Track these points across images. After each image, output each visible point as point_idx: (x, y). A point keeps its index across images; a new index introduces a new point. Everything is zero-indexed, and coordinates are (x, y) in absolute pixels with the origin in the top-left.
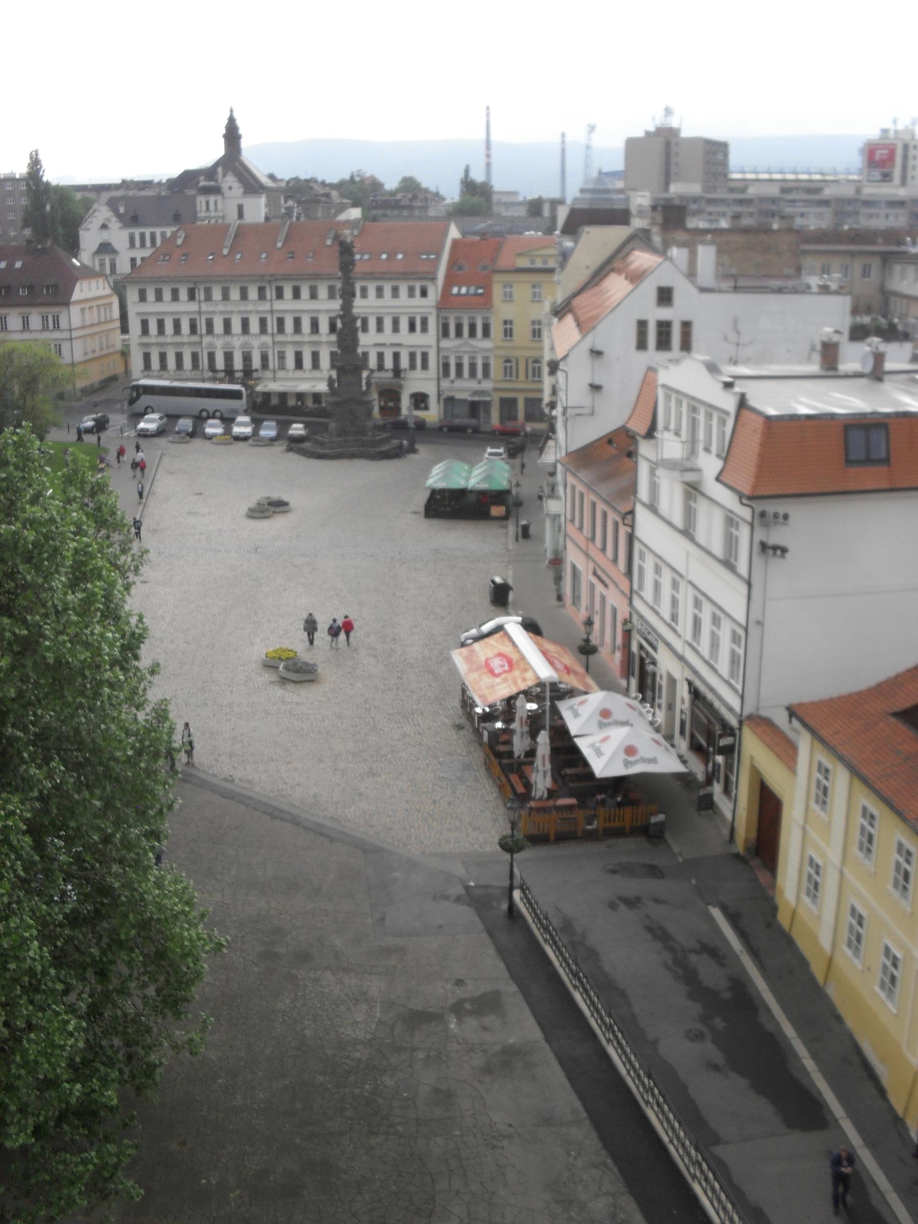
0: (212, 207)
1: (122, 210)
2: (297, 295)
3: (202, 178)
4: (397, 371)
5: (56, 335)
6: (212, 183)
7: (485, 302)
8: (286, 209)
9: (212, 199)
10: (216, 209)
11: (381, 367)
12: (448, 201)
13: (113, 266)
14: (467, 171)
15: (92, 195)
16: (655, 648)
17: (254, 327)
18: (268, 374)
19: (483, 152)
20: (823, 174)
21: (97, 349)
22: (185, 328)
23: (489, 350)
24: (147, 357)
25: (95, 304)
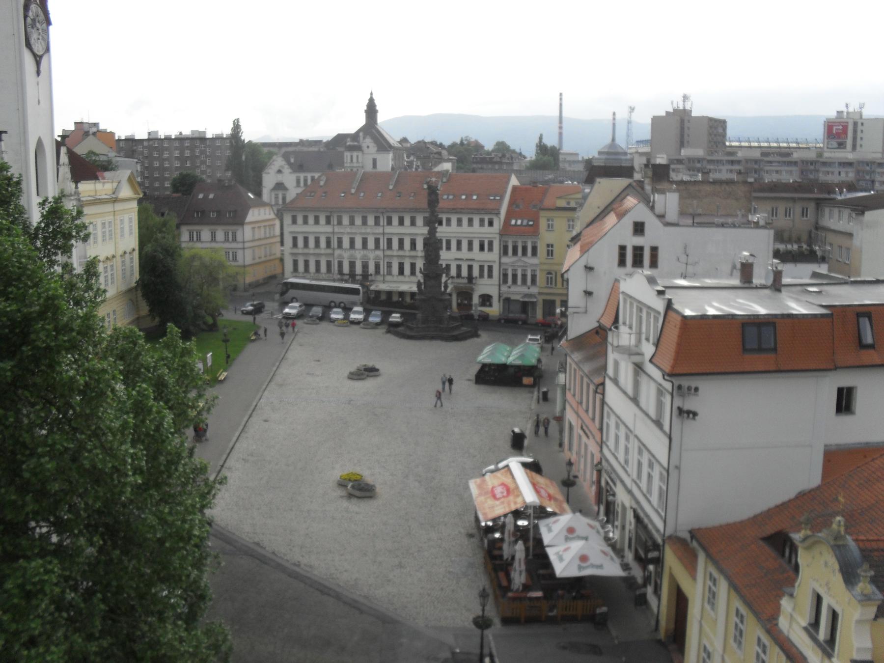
0: (355, 160)
1: (292, 160)
2: (401, 222)
3: (349, 139)
4: (470, 278)
5: (234, 245)
6: (356, 143)
7: (534, 230)
8: (407, 162)
9: (355, 154)
11: (459, 275)
12: (528, 159)
14: (541, 138)
15: (272, 149)
16: (615, 484)
17: (371, 244)
18: (380, 278)
19: (557, 124)
20: (797, 143)
22: (323, 244)
23: (536, 265)
24: (295, 263)
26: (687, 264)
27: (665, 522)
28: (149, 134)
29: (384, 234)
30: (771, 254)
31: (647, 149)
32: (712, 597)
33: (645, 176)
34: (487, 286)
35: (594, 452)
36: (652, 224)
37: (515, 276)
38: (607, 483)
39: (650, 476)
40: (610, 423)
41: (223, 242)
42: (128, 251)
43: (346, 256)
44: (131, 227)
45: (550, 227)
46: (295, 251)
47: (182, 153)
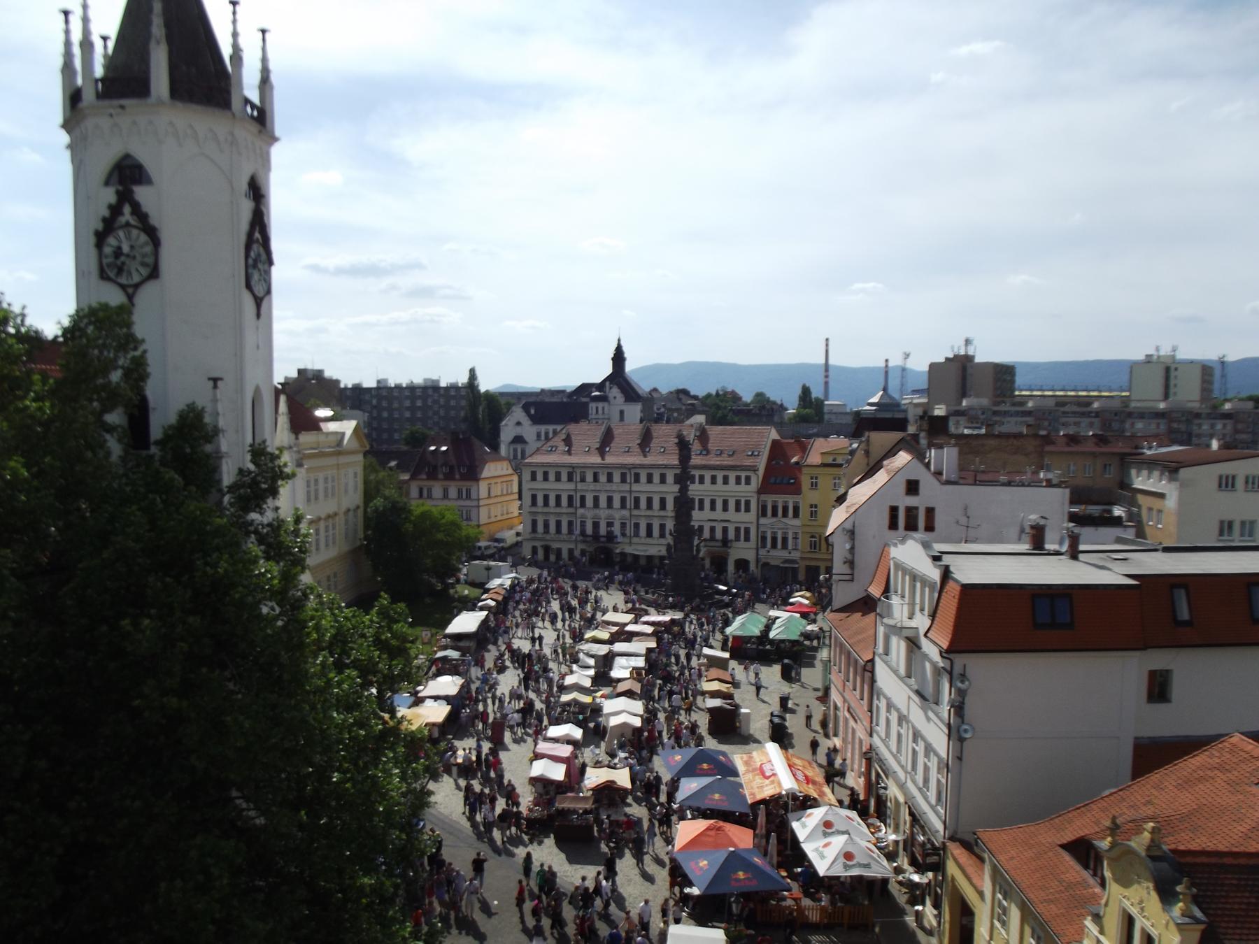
1: (533, 412)
5: (468, 503)
8: (658, 414)
9: (600, 405)
10: (603, 413)
11: (712, 538)
13: (523, 452)
19: (823, 374)
21: (499, 514)
22: (564, 502)
25: (499, 480)
26: (968, 527)
27: (945, 823)
28: (379, 382)
29: (631, 492)
30: (1066, 517)
31: (924, 400)
32: (1001, 916)
33: (920, 429)
34: (744, 550)
35: (862, 737)
36: (928, 483)
37: (774, 540)
38: (878, 775)
39: (926, 769)
40: (880, 705)
41: (456, 499)
42: (352, 507)
43: (588, 514)
44: (356, 482)
45: (814, 486)
46: (534, 509)
47: (413, 402)
